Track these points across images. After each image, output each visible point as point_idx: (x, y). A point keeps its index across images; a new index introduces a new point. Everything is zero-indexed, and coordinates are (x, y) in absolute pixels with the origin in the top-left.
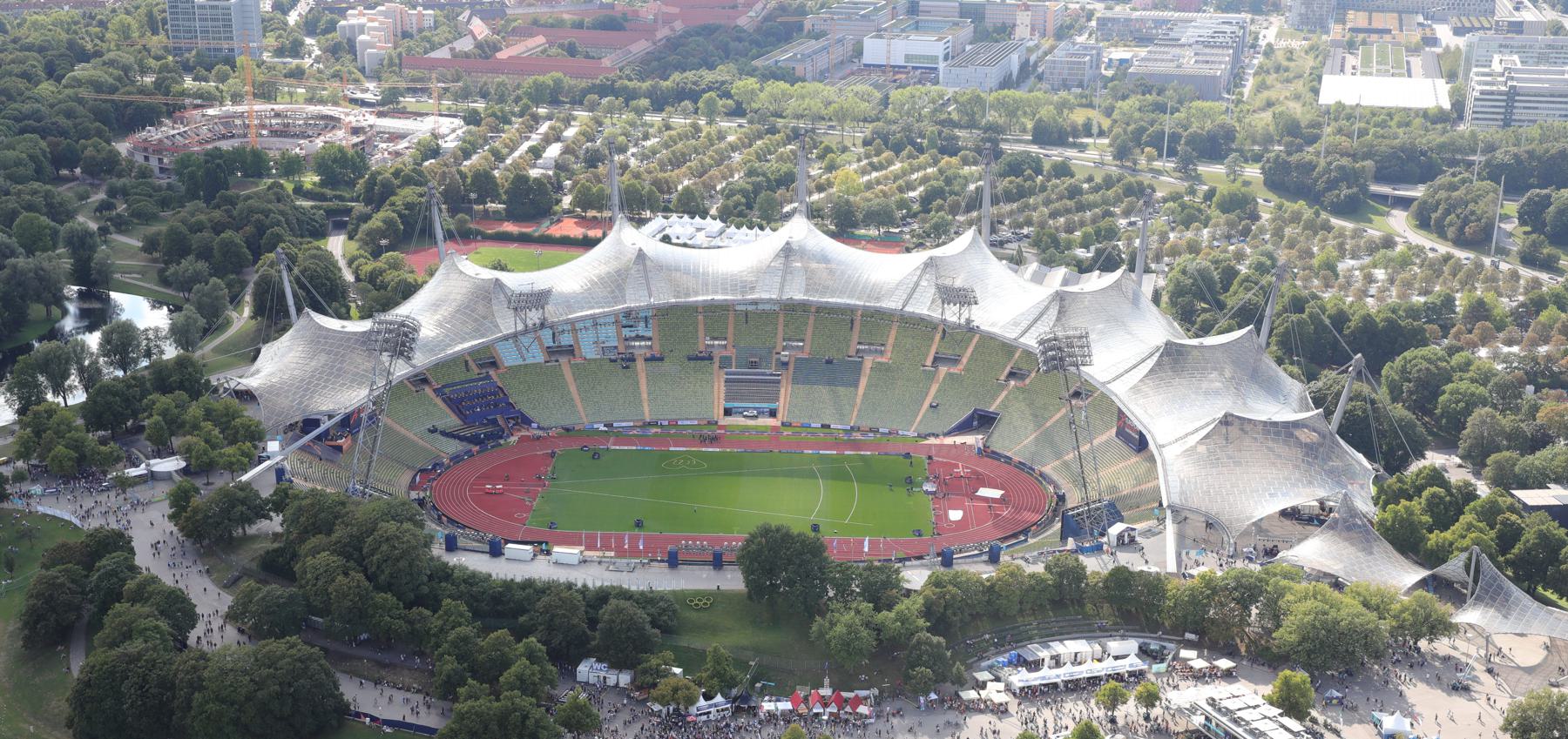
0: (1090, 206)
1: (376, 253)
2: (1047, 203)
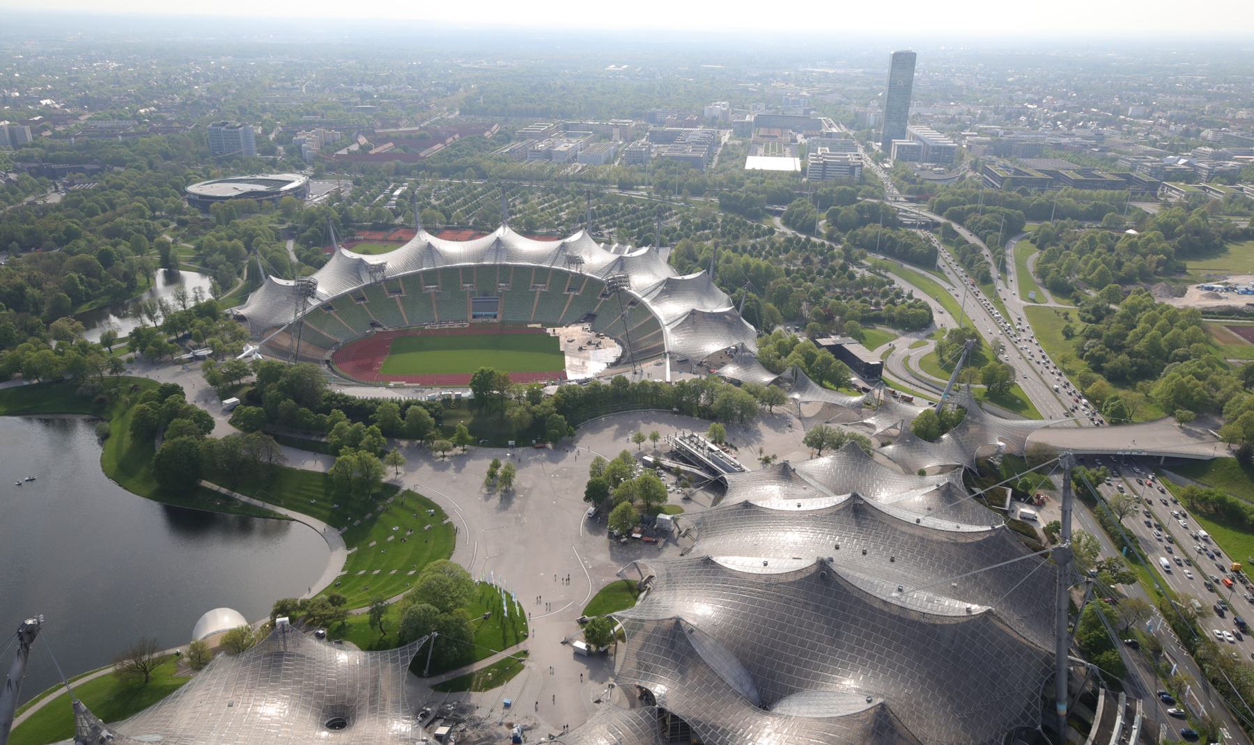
0: (643, 216)
1: (309, 247)
2: (623, 215)
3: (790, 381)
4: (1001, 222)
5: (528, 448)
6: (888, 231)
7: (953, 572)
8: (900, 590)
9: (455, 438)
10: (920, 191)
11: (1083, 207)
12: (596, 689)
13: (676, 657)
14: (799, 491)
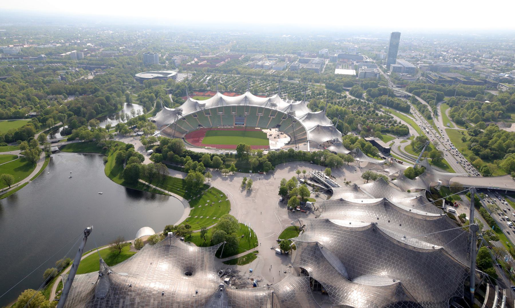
0: (297, 90)
2: (290, 89)
3: (355, 153)
4: (435, 96)
5: (257, 174)
6: (391, 98)
7: (425, 231)
8: (405, 237)
9: (230, 169)
10: (402, 84)
11: (468, 91)
12: (284, 268)
13: (316, 257)
14: (361, 196)
